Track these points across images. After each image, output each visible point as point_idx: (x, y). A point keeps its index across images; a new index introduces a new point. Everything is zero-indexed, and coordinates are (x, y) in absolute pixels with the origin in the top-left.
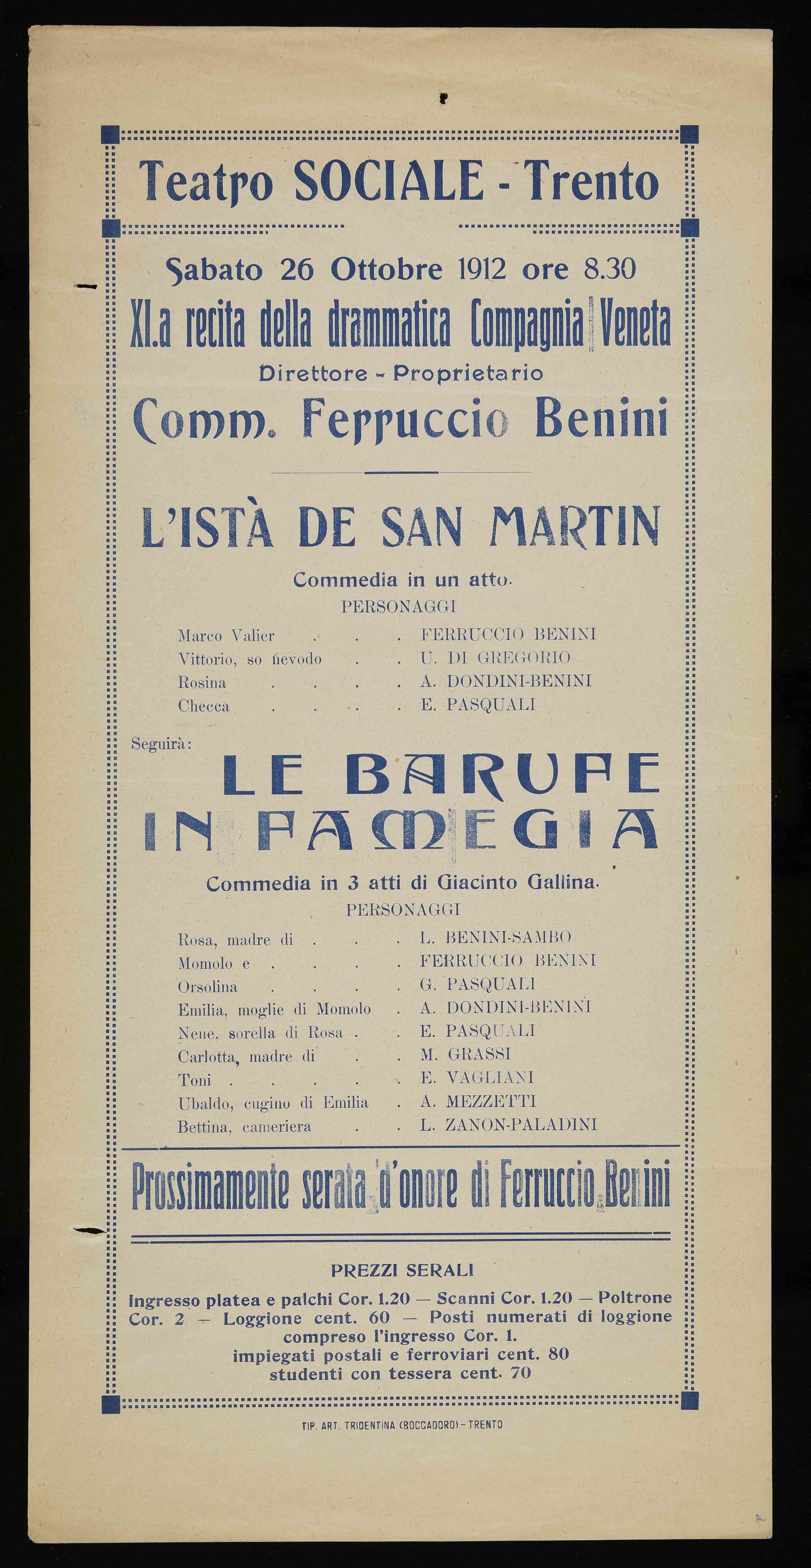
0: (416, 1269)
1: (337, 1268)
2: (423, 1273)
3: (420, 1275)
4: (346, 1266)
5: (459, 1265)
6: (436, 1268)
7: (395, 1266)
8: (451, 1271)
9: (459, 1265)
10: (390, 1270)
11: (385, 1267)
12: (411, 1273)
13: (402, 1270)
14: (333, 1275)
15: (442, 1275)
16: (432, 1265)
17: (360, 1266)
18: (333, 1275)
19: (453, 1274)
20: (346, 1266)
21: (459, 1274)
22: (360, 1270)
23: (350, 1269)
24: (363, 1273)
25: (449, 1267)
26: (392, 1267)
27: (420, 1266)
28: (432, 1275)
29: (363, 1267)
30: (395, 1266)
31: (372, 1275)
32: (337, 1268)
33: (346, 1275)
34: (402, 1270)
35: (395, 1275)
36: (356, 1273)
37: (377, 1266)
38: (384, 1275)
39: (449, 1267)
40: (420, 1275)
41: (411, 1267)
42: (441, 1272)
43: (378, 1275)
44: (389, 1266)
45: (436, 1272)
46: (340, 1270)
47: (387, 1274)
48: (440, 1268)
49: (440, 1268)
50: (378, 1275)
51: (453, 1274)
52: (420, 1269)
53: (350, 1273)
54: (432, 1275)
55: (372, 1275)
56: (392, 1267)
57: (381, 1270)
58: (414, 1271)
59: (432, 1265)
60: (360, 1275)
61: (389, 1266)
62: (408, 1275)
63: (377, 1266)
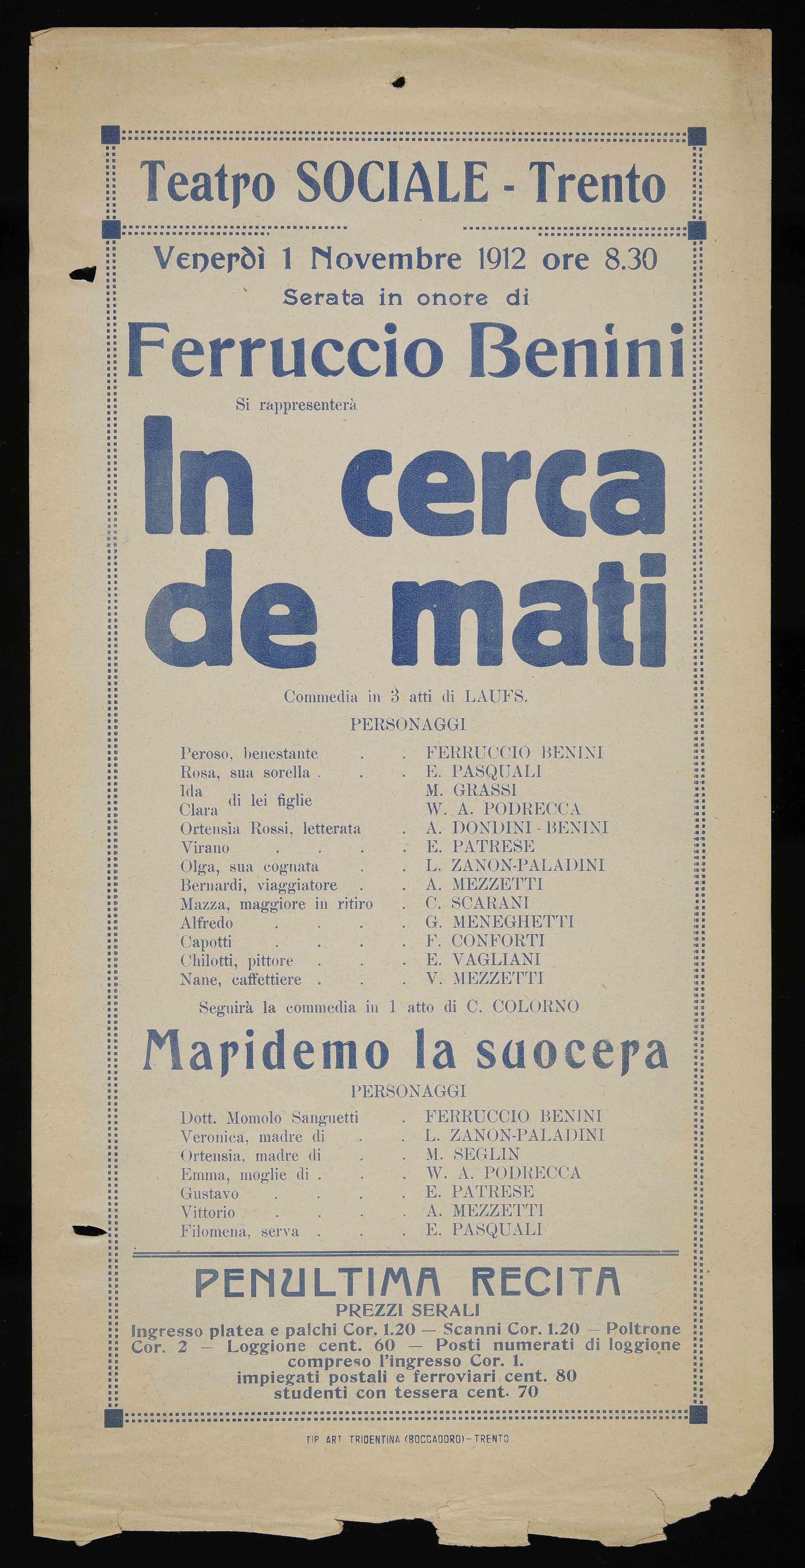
0: (422, 1309)
2: (429, 1313)
3: (425, 1314)
4: (351, 1305)
5: (465, 1306)
6: (442, 1308)
8: (457, 1311)
9: (465, 1306)
11: (390, 1307)
12: (417, 1313)
16: (438, 1305)
17: (365, 1306)
19: (459, 1315)
20: (351, 1305)
21: (465, 1314)
22: (365, 1310)
23: (355, 1308)
24: (368, 1313)
25: (455, 1307)
26: (397, 1307)
27: (425, 1306)
28: (438, 1315)
29: (367, 1307)
30: (400, 1305)
31: (377, 1314)
33: (351, 1315)
35: (400, 1314)
36: (361, 1312)
37: (382, 1306)
38: (389, 1315)
39: (455, 1307)
40: (425, 1314)
42: (447, 1313)
43: (383, 1315)
44: (395, 1305)
46: (345, 1310)
48: (446, 1308)
49: (446, 1308)
50: (383, 1315)
51: (459, 1315)
52: (425, 1310)
56: (397, 1307)
57: (386, 1310)
58: (419, 1311)
59: (438, 1305)
61: (395, 1305)
62: (413, 1314)
63: (382, 1306)
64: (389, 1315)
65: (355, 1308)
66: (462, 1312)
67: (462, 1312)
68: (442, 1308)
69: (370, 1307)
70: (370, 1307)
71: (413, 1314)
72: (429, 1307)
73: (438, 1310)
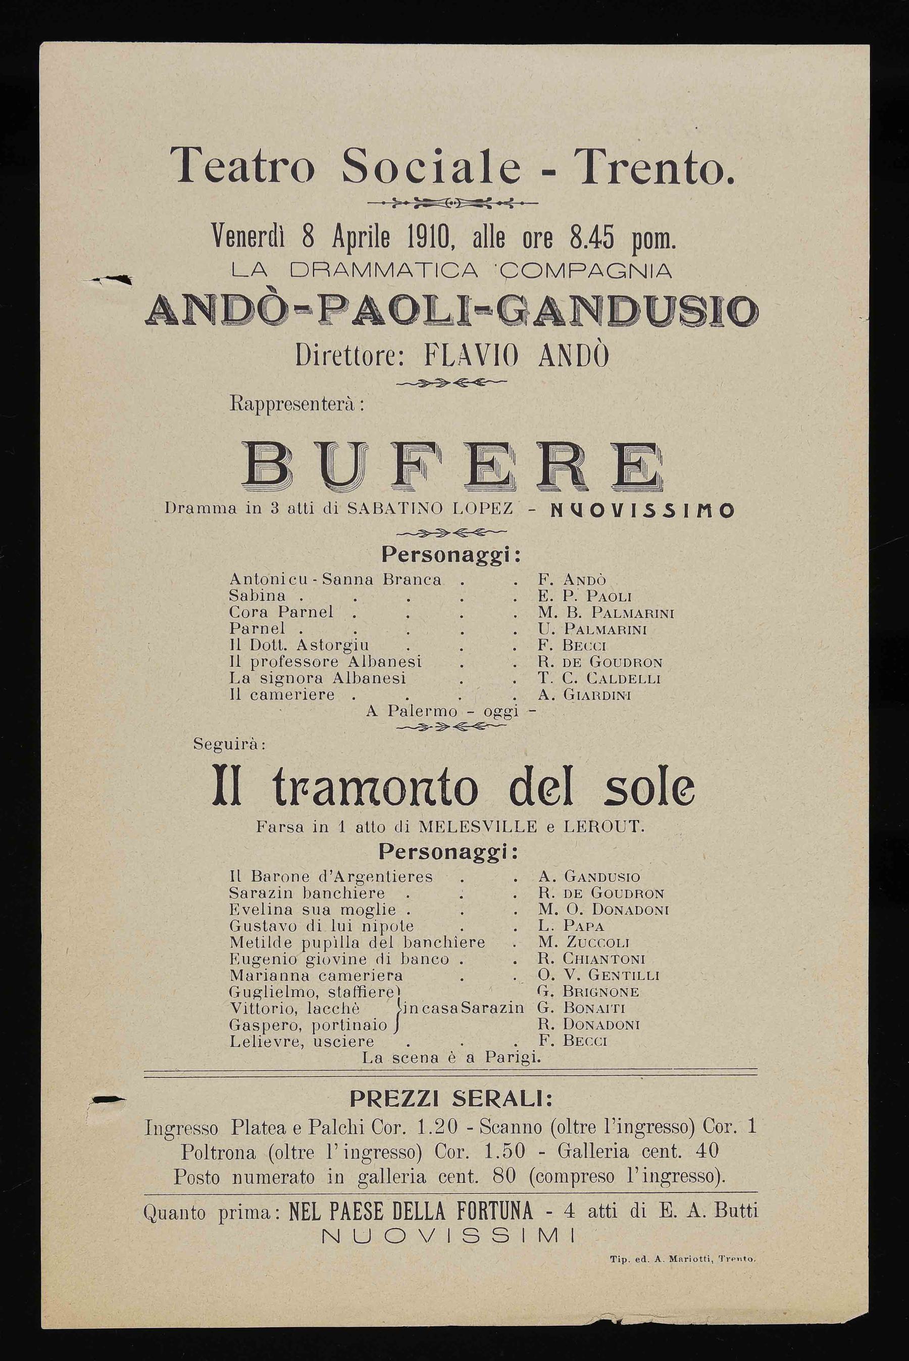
1: (358, 1096)
2: (475, 1102)
4: (370, 1093)
6: (493, 1095)
7: (436, 1092)
8: (513, 1100)
9: (523, 1092)
10: (430, 1098)
11: (423, 1094)
12: (459, 1102)
13: (446, 1098)
15: (500, 1104)
16: (488, 1092)
17: (387, 1092)
20: (370, 1093)
21: (523, 1104)
22: (387, 1098)
23: (374, 1096)
24: (392, 1102)
27: (471, 1092)
28: (488, 1104)
29: (391, 1094)
30: (436, 1092)
31: (405, 1105)
32: (358, 1096)
33: (370, 1105)
34: (446, 1098)
35: (436, 1104)
36: (382, 1102)
37: (412, 1092)
38: (420, 1105)
39: (511, 1094)
40: (471, 1104)
41: (459, 1094)
43: (413, 1105)
44: (427, 1092)
45: (493, 1101)
48: (498, 1095)
49: (498, 1095)
50: (413, 1105)
51: (515, 1104)
53: (375, 1101)
54: (488, 1104)
55: (405, 1105)
57: (416, 1098)
58: (464, 1100)
59: (488, 1092)
60: (387, 1104)
62: (455, 1104)
64: (420, 1105)
66: (518, 1100)
67: (518, 1100)
68: (493, 1095)
69: (395, 1094)
70: (395, 1094)
71: (455, 1104)
72: (475, 1094)
73: (488, 1099)
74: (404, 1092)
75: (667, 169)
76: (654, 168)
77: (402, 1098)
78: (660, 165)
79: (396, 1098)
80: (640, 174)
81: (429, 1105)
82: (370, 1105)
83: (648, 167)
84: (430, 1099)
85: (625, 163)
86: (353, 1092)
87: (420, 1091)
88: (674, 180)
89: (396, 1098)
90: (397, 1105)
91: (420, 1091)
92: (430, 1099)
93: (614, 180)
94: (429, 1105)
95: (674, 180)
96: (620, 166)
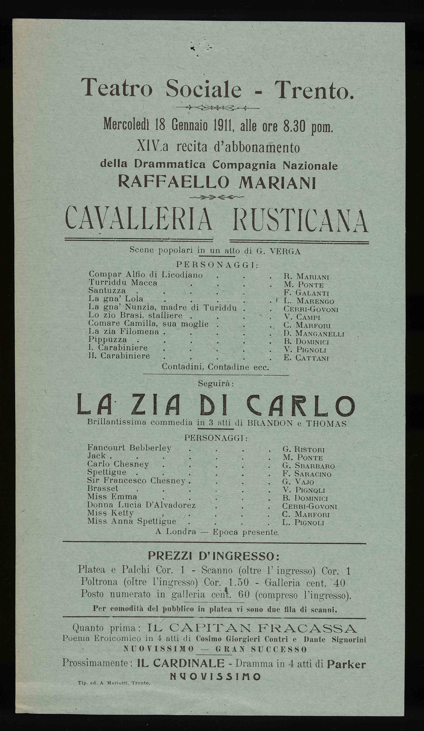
1: (152, 554)
4: (158, 552)
7: (191, 553)
14: (149, 558)
17: (167, 552)
18: (149, 558)
20: (158, 552)
23: (160, 554)
24: (169, 557)
26: (188, 555)
29: (168, 553)
30: (191, 553)
31: (175, 559)
32: (152, 554)
33: (158, 559)
35: (191, 559)
36: (164, 557)
37: (179, 553)
38: (183, 559)
43: (179, 559)
44: (186, 553)
47: (185, 558)
50: (179, 559)
53: (161, 557)
55: (175, 559)
56: (188, 555)
57: (181, 555)
60: (166, 558)
64: (183, 559)
65: (160, 554)
74: (175, 552)
75: (321, 92)
76: (314, 91)
77: (174, 555)
78: (317, 89)
79: (171, 555)
80: (307, 94)
81: (187, 559)
82: (158, 559)
83: (311, 90)
84: (188, 556)
85: (300, 88)
86: (149, 552)
87: (183, 552)
88: (324, 97)
89: (171, 555)
90: (171, 559)
91: (183, 552)
92: (188, 556)
93: (295, 97)
94: (187, 559)
95: (324, 97)
96: (297, 90)
